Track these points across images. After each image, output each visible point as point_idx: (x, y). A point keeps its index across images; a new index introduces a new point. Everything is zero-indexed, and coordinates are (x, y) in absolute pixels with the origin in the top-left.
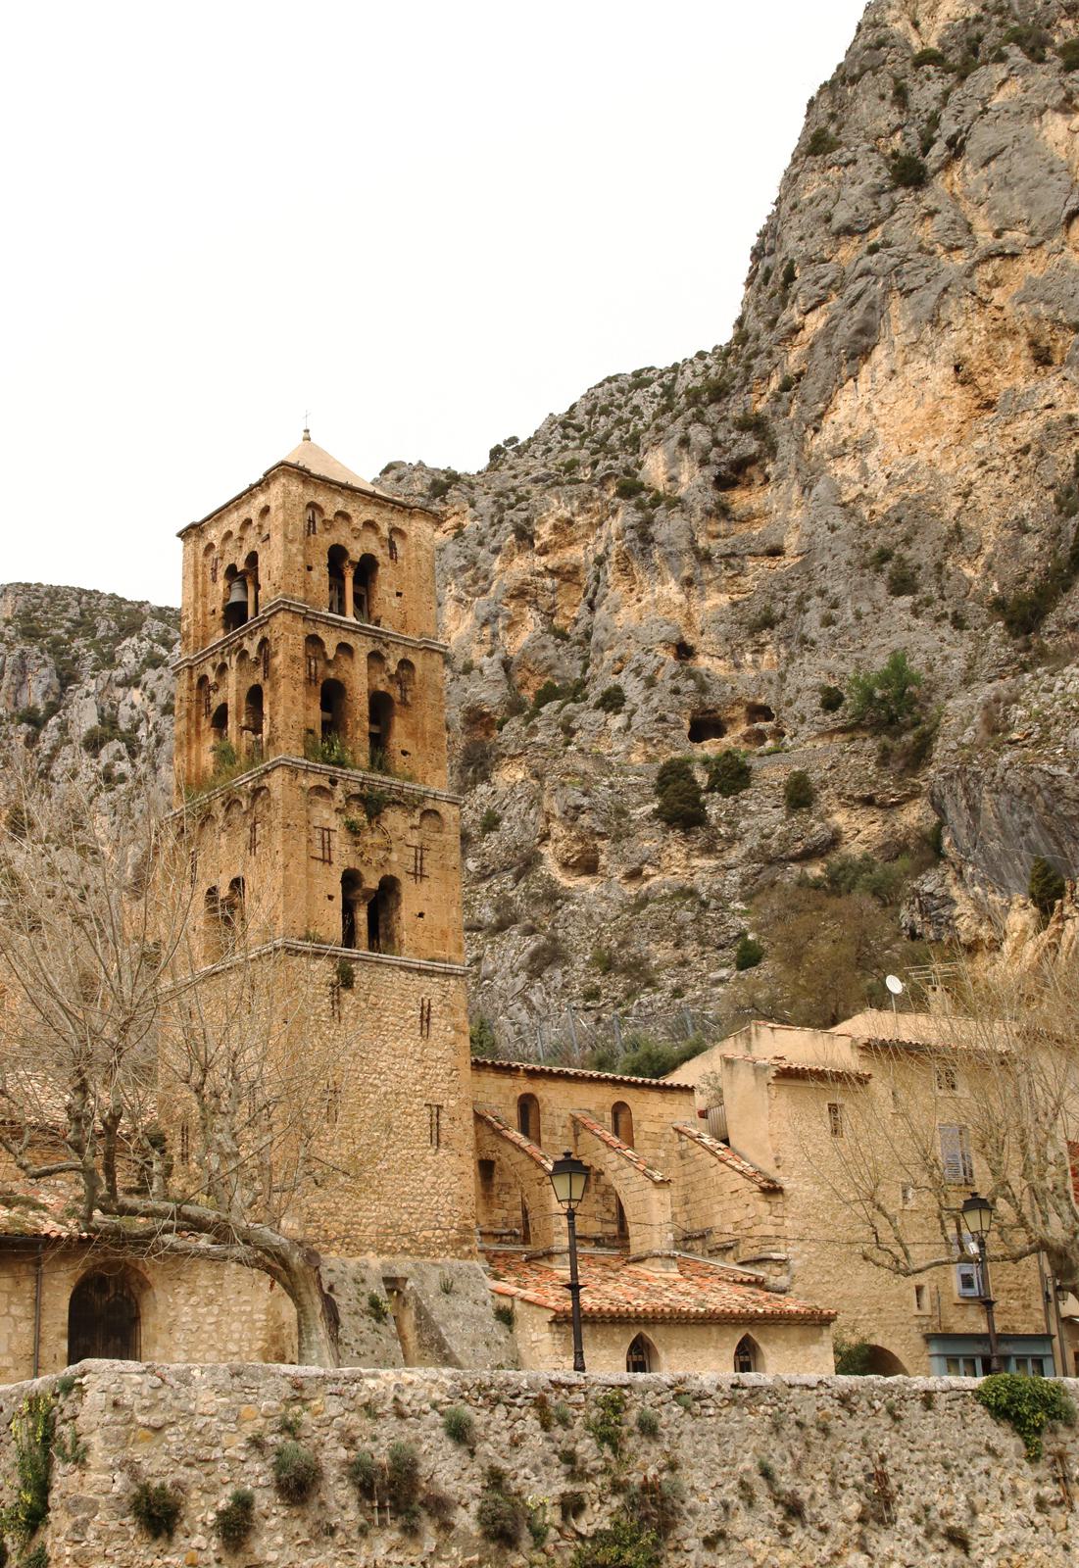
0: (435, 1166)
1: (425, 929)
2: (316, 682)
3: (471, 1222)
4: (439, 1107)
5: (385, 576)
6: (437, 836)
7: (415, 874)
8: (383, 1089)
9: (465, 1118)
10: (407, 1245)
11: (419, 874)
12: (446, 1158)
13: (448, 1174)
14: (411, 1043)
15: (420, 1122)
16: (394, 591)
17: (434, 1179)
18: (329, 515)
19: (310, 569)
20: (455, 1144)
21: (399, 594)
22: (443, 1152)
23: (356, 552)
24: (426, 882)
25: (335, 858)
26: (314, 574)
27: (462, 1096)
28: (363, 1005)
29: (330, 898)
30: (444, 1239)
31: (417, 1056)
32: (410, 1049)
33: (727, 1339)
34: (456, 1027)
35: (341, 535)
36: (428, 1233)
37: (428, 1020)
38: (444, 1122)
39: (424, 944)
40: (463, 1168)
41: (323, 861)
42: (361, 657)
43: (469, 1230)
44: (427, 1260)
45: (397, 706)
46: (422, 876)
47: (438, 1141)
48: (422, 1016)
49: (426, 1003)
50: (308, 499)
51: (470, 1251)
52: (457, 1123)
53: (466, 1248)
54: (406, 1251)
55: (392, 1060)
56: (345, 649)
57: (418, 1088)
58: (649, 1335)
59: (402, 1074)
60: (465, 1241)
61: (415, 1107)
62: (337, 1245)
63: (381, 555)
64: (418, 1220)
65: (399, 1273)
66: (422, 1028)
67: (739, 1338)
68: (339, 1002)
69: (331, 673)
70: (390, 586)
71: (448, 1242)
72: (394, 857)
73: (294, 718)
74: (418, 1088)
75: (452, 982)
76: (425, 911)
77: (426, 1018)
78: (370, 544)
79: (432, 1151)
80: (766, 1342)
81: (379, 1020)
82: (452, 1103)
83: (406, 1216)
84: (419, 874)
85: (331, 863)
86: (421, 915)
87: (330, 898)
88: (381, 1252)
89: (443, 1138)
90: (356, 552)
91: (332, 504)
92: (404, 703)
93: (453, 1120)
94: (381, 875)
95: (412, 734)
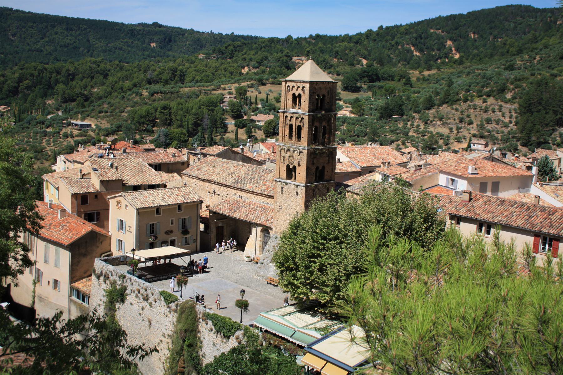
11: (299, 165)
14: (294, 198)
35: (294, 91)
42: (295, 118)
50: (287, 85)
56: (292, 117)
63: (302, 93)
77: (297, 195)
78: (299, 91)
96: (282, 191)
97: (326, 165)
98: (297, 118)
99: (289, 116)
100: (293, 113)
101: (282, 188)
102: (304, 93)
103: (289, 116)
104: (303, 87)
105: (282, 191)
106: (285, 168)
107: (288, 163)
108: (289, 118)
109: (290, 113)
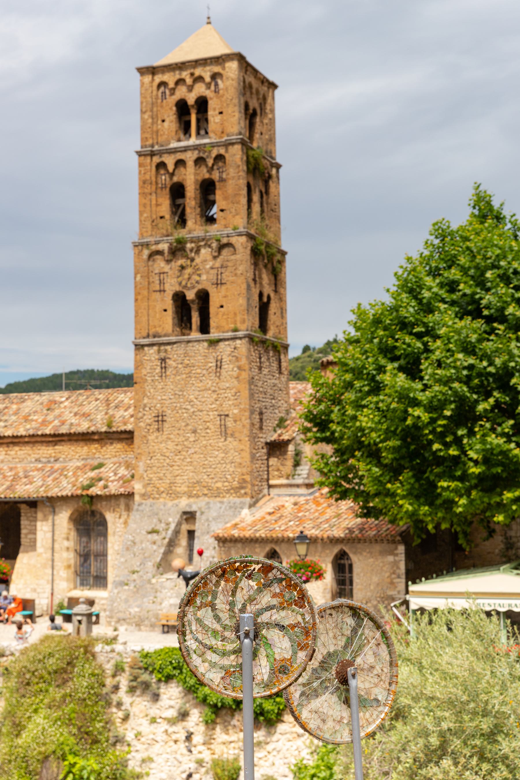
0: (224, 448)
1: (223, 315)
2: (166, 187)
3: (248, 478)
4: (227, 415)
5: (213, 106)
6: (233, 257)
7: (217, 284)
8: (192, 410)
9: (243, 418)
10: (206, 492)
12: (232, 444)
13: (232, 451)
15: (213, 427)
16: (217, 112)
17: (223, 455)
18: (171, 85)
19: (163, 121)
20: (237, 435)
21: (221, 113)
22: (229, 439)
23: (191, 99)
24: (224, 287)
25: (167, 287)
26: (166, 124)
27: (242, 407)
28: (180, 366)
29: (165, 310)
30: (229, 488)
31: (213, 388)
32: (209, 386)
33: (328, 551)
34: (239, 368)
35: (181, 92)
36: (219, 485)
37: (220, 368)
38: (230, 423)
39: (223, 323)
40: (242, 447)
41: (160, 291)
42: (190, 164)
43: (244, 481)
44: (218, 499)
45: (217, 184)
46: (221, 284)
47: (226, 433)
48: (217, 365)
49: (219, 358)
51: (245, 493)
52: (238, 423)
53: (243, 491)
54: (206, 495)
55: (197, 393)
56: (180, 163)
57: (213, 406)
58: (277, 549)
59: (203, 400)
60: (242, 488)
61: (212, 417)
62: (164, 495)
63: (208, 93)
64: (213, 478)
65: (194, 508)
66: (216, 373)
67: (336, 550)
68: (165, 367)
69: (175, 179)
70: (214, 109)
71: (232, 489)
72: (204, 277)
73: (145, 215)
74: (213, 406)
75: (238, 342)
76: (224, 304)
79: (223, 440)
80: (355, 553)
81: (190, 373)
82: (236, 411)
83: (205, 477)
84: (219, 283)
85: (164, 291)
86: (222, 307)
87: (165, 310)
88: (190, 496)
89: (229, 432)
90: (191, 99)
91: (170, 78)
92: (222, 180)
93: (235, 421)
94: (195, 291)
95: (226, 198)
96: (164, 368)
97: (272, 295)
98: (199, 161)
99: (170, 161)
100: (185, 149)
101: (163, 360)
102: (216, 91)
103: (170, 161)
104: (214, 76)
105: (164, 368)
106: (169, 304)
107: (178, 288)
108: (171, 168)
109: (174, 151)
